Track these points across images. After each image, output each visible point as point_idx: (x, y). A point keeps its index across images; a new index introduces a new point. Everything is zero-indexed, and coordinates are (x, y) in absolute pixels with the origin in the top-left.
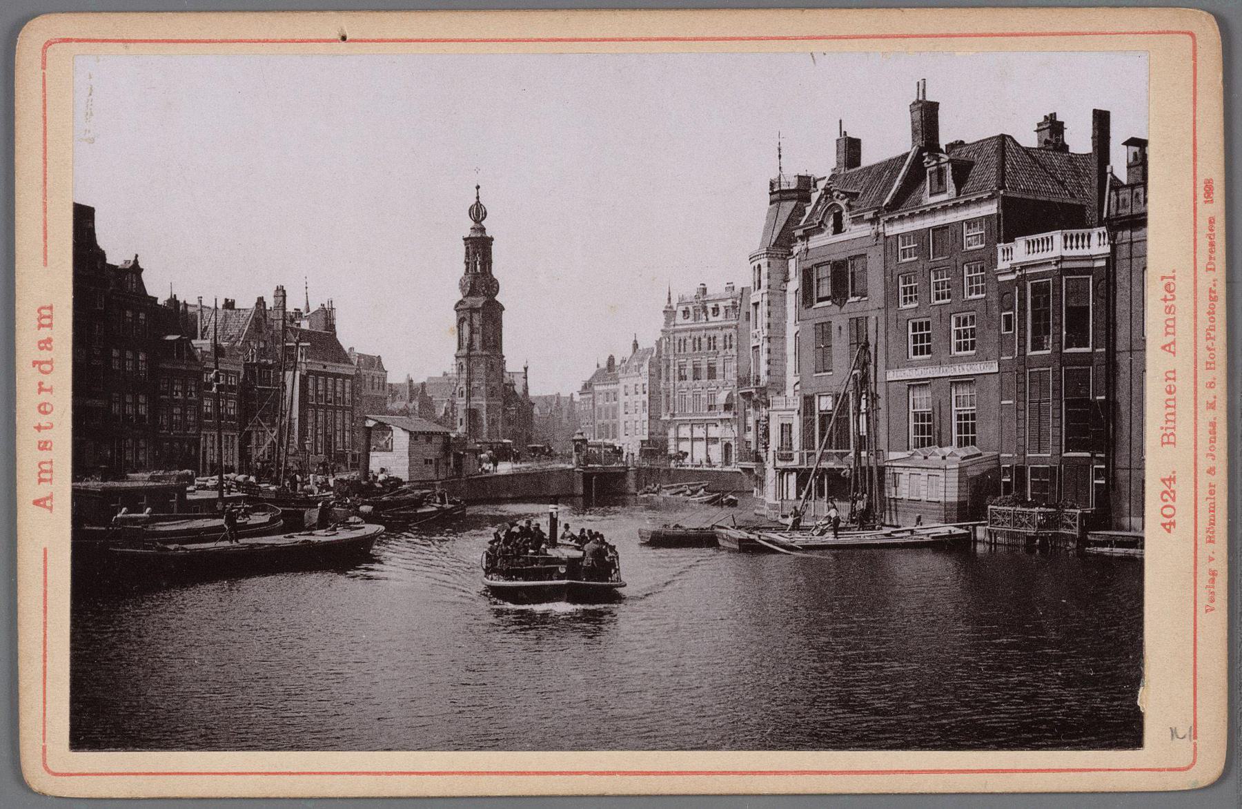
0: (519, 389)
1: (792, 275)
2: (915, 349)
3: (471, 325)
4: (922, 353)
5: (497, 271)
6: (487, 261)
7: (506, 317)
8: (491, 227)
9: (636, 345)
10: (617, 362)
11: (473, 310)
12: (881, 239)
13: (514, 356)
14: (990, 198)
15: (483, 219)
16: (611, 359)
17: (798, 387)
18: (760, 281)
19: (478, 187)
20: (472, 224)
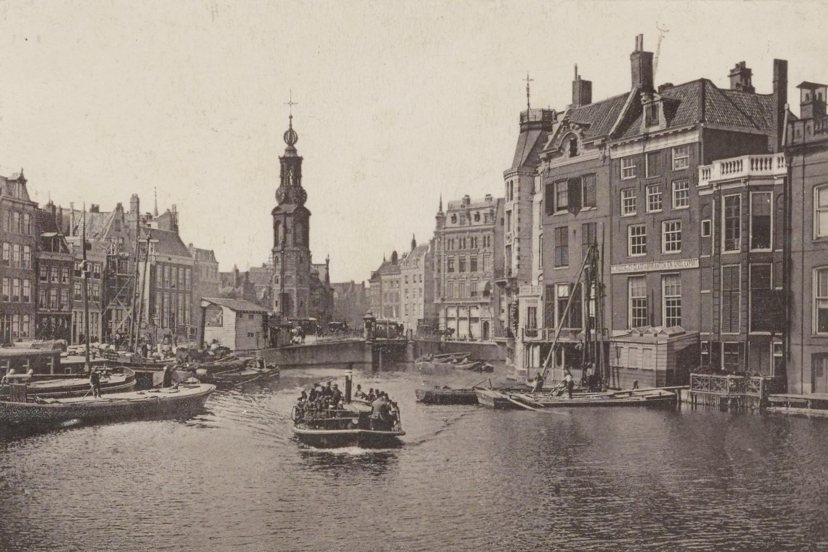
0: (322, 278)
1: (537, 189)
2: (634, 248)
3: (285, 227)
4: (639, 252)
5: (305, 184)
6: (298, 176)
7: (312, 220)
8: (301, 148)
9: (414, 243)
10: (400, 257)
11: (286, 215)
12: (607, 162)
13: (319, 249)
14: (693, 129)
16: (395, 255)
17: (541, 278)
19: (291, 117)
20: (286, 146)
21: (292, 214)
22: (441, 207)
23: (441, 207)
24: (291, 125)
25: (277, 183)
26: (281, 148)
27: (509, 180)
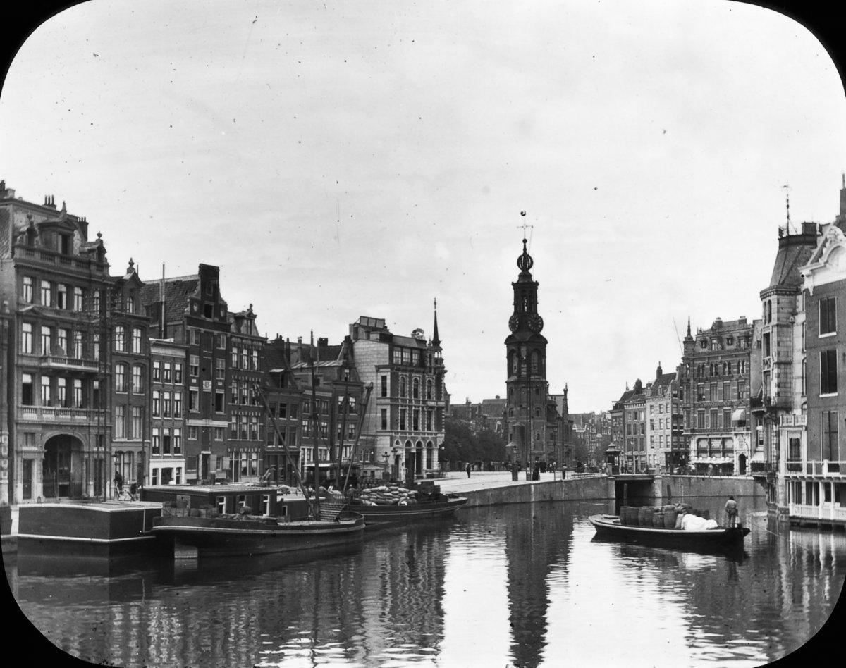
0: (560, 409)
1: (800, 309)
5: (542, 311)
9: (659, 370)
10: (644, 386)
15: (530, 267)
16: (639, 383)
17: (805, 406)
18: (770, 315)
19: (525, 241)
20: (521, 271)
21: (526, 341)
22: (689, 331)
23: (689, 331)
24: (525, 249)
25: (510, 310)
26: (515, 273)
27: (767, 300)
